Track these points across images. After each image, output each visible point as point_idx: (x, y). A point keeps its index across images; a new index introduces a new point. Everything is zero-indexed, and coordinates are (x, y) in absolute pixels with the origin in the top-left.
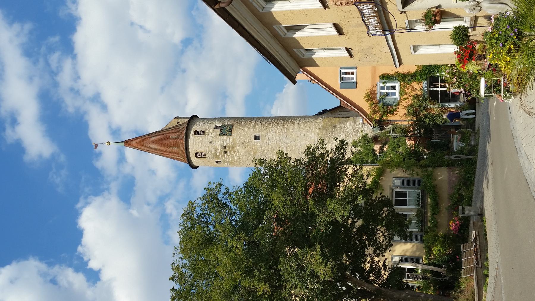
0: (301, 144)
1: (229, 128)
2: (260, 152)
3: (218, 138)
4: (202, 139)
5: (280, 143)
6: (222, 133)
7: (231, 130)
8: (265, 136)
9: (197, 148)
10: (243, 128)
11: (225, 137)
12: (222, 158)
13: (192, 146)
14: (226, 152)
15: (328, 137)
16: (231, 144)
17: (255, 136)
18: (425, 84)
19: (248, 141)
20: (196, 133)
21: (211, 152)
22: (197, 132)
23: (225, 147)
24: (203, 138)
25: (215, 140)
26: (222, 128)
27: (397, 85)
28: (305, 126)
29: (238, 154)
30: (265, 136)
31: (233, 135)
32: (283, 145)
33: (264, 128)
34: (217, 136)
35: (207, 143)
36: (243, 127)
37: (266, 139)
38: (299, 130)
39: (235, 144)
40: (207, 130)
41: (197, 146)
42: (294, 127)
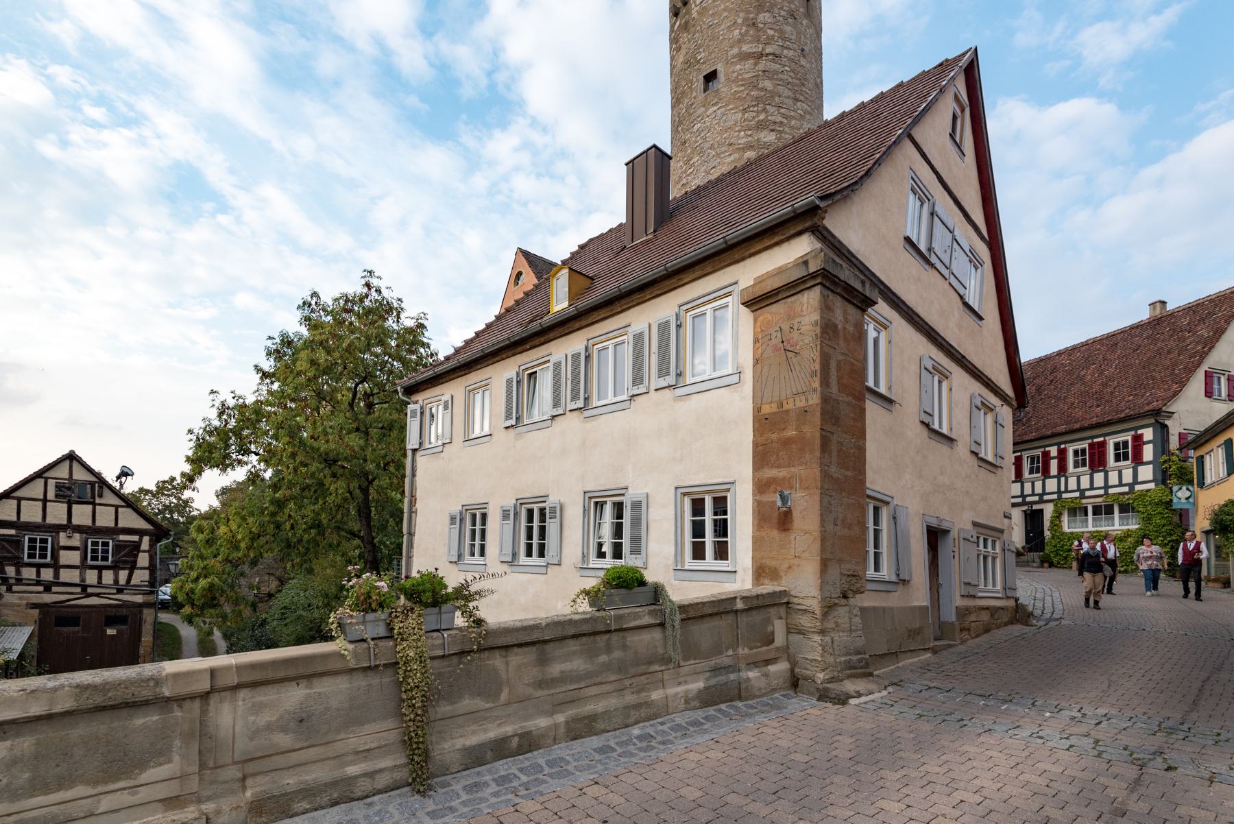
33: (743, 88)
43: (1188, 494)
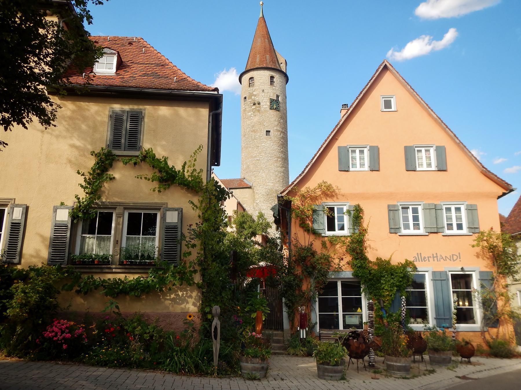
0: (262, 173)
1: (277, 108)
5: (263, 154)
6: (272, 101)
8: (270, 140)
10: (277, 120)
11: (269, 104)
12: (250, 102)
14: (254, 104)
15: (269, 198)
16: (262, 109)
18: (348, 273)
20: (272, 78)
21: (254, 91)
23: (259, 104)
26: (277, 101)
27: (346, 232)
28: (279, 177)
30: (270, 140)
31: (271, 111)
32: (261, 157)
35: (263, 87)
38: (276, 171)
41: (260, 78)
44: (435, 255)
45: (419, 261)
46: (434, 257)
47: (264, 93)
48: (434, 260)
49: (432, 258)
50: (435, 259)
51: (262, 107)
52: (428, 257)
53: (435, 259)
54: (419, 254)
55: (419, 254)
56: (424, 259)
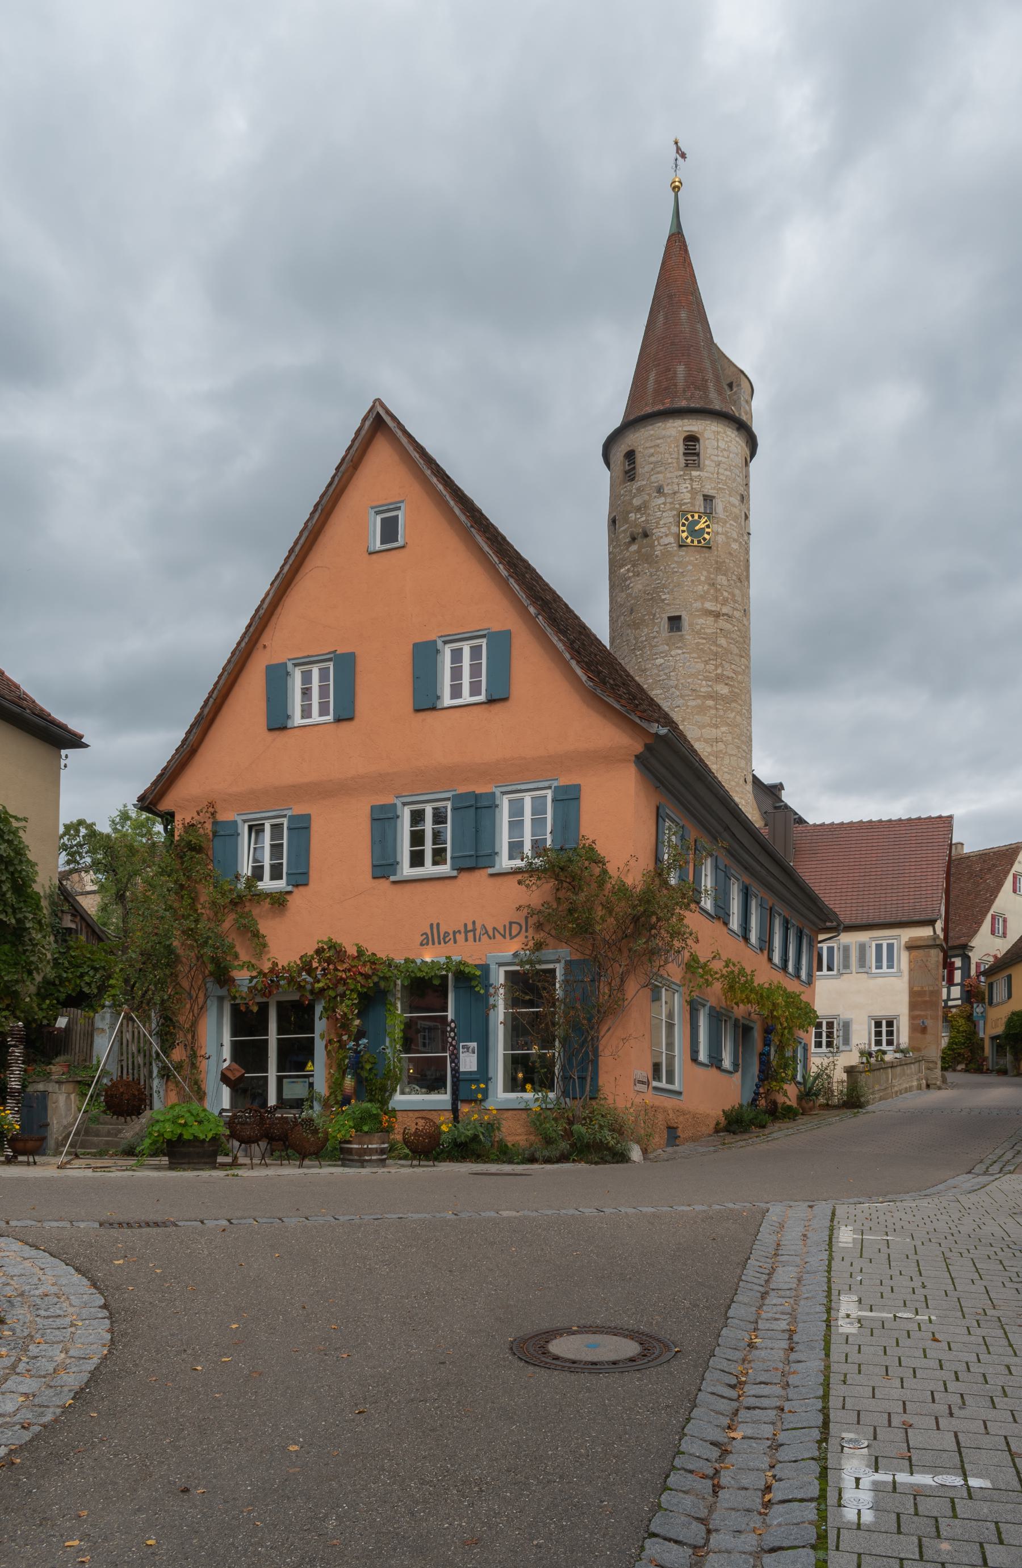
2: (636, 638)
3: (671, 510)
4: (670, 461)
7: (696, 543)
8: (678, 645)
9: (646, 452)
10: (703, 578)
12: (624, 531)
13: (652, 435)
14: (634, 539)
17: (678, 618)
19: (663, 597)
21: (634, 497)
22: (695, 445)
23: (646, 535)
24: (675, 465)
25: (669, 500)
29: (631, 574)
33: (704, 641)
34: (679, 504)
36: (708, 578)
37: (670, 650)
39: (656, 562)
40: (698, 473)
41: (652, 450)
42: (704, 727)
43: (982, 1010)
44: (470, 927)
45: (433, 944)
46: (466, 932)
47: (664, 495)
48: (466, 940)
49: (463, 934)
50: (470, 935)
51: (656, 543)
52: (454, 933)
53: (470, 935)
54: (435, 926)
55: (435, 926)
56: (444, 938)
